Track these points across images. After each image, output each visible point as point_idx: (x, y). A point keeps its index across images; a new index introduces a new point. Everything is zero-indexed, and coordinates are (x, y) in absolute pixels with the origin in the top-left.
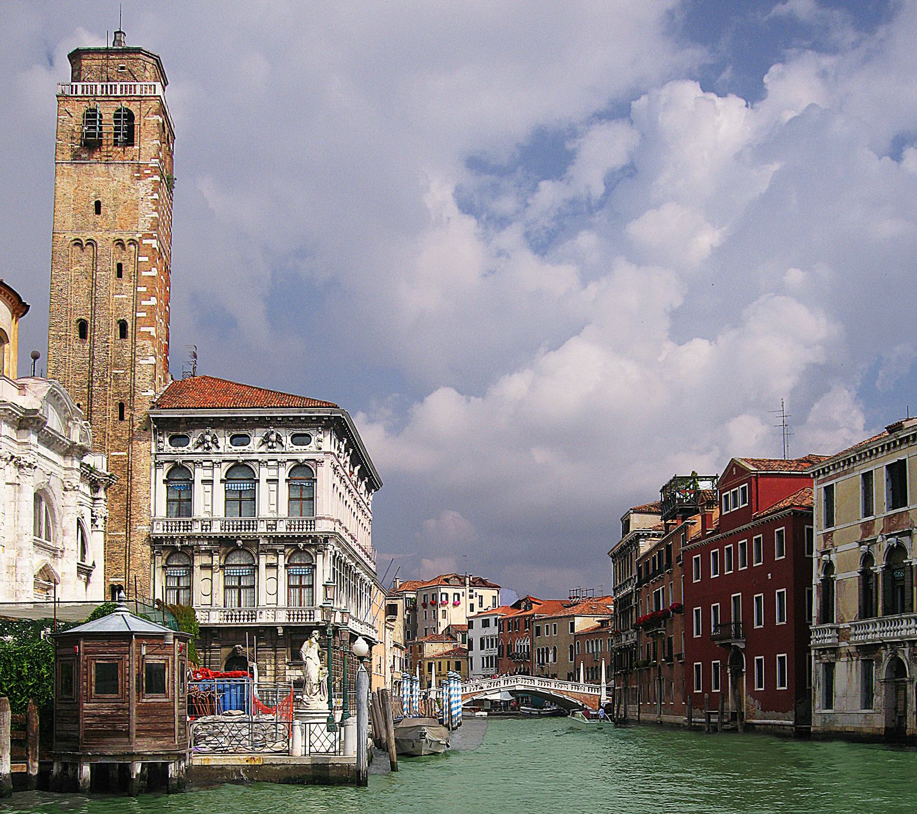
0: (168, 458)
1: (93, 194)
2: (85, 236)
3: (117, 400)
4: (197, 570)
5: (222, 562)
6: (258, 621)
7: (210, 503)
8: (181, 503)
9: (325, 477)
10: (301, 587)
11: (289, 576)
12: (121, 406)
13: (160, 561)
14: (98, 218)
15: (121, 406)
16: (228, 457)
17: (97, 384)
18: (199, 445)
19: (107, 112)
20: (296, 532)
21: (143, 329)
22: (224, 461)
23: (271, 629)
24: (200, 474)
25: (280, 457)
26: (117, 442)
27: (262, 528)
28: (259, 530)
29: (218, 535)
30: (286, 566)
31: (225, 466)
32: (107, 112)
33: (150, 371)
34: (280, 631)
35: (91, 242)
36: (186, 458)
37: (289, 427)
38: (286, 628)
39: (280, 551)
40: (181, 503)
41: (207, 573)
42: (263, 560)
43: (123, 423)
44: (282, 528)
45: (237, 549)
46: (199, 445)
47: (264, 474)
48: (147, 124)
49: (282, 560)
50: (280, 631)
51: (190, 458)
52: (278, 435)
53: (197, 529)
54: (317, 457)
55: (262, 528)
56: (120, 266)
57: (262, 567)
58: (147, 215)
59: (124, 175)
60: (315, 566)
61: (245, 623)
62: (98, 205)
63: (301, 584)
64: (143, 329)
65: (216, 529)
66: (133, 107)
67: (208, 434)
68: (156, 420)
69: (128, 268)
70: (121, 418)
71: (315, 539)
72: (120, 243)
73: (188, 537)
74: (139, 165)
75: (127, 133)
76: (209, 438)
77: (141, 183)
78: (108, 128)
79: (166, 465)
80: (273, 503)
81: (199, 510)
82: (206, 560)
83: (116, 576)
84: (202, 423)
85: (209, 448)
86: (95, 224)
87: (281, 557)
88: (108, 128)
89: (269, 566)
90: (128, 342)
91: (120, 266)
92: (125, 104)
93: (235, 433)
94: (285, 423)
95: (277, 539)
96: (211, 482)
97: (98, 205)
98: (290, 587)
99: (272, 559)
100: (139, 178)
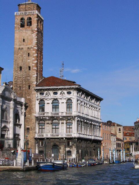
0: (39, 98)
1: (23, 38)
2: (22, 47)
4: (46, 124)
5: (51, 122)
7: (49, 109)
8: (42, 108)
9: (74, 101)
10: (69, 128)
11: (67, 125)
12: (29, 86)
13: (37, 122)
14: (24, 43)
15: (29, 86)
16: (53, 97)
18: (46, 95)
19: (26, 18)
20: (68, 115)
21: (34, 68)
22: (52, 98)
23: (62, 138)
24: (46, 102)
25: (64, 97)
26: (28, 95)
27: (60, 114)
30: (66, 123)
31: (52, 100)
32: (26, 18)
33: (35, 78)
34: (64, 139)
35: (22, 48)
36: (43, 98)
37: (66, 90)
38: (66, 138)
40: (42, 108)
41: (47, 125)
42: (61, 122)
44: (64, 114)
45: (55, 119)
46: (46, 95)
47: (60, 101)
48: (34, 20)
49: (65, 122)
50: (64, 139)
51: (44, 98)
52: (64, 92)
53: (46, 115)
54: (73, 97)
55: (60, 114)
56: (29, 54)
57: (60, 123)
58: (35, 41)
59: (29, 32)
60: (72, 123)
61: (56, 137)
62: (24, 40)
63: (69, 128)
64: (34, 68)
65: (50, 115)
66: (31, 17)
67: (48, 92)
68: (37, 89)
69: (31, 54)
70: (29, 89)
71: (72, 116)
72: (28, 48)
73: (44, 117)
74: (33, 30)
75: (30, 23)
76: (48, 93)
77: (33, 34)
78: (26, 22)
80: (62, 109)
81: (46, 110)
82: (47, 122)
83: (28, 126)
84: (46, 90)
85: (48, 95)
86: (23, 44)
87: (65, 121)
88: (26, 22)
89: (62, 123)
90: (31, 71)
91: (29, 54)
92: (29, 16)
93: (54, 91)
94: (65, 89)
96: (48, 103)
97: (24, 40)
98: (67, 128)
99: (63, 122)
100: (33, 33)
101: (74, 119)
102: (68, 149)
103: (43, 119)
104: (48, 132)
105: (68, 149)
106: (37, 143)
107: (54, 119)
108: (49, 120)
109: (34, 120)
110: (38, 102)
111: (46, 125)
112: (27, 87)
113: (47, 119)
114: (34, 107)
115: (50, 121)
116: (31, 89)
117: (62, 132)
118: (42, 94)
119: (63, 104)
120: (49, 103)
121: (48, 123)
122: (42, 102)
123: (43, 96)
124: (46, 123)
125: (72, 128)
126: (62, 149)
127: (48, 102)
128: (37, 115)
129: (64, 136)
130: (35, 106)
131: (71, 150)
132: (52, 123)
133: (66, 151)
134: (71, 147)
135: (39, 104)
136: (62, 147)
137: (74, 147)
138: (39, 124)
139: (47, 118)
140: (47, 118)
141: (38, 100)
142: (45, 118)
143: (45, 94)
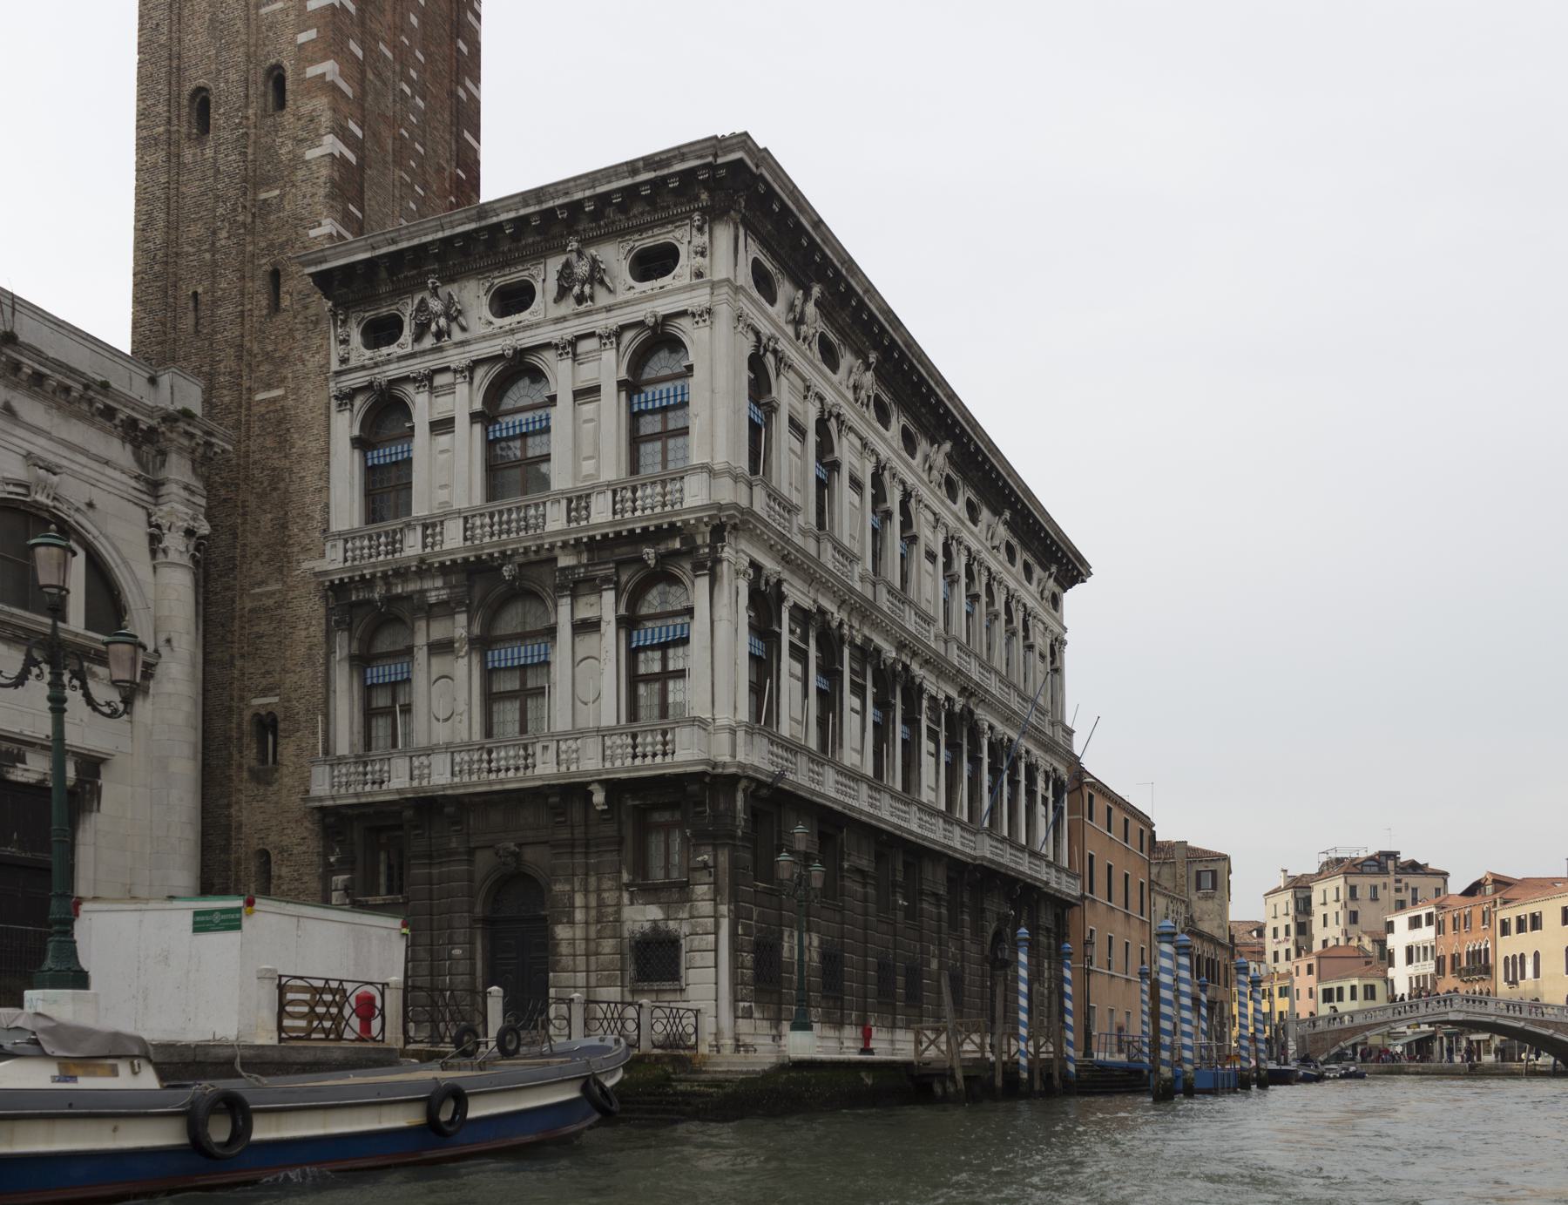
3: (265, 263)
4: (421, 655)
6: (539, 771)
8: (386, 488)
17: (224, 234)
23: (574, 792)
24: (423, 407)
26: (265, 368)
28: (551, 526)
29: (459, 557)
34: (599, 798)
36: (394, 371)
39: (606, 580)
40: (386, 488)
43: (279, 320)
49: (606, 606)
50: (599, 798)
61: (511, 780)
70: (275, 306)
73: (401, 573)
79: (359, 401)
83: (265, 692)
87: (609, 597)
95: (596, 546)
96: (442, 426)
101: (710, 567)
102: (642, 916)
103: (391, 600)
104: (444, 735)
105: (642, 916)
106: (346, 864)
107: (502, 594)
108: (445, 609)
109: (310, 610)
110: (344, 426)
111: (422, 668)
112: (258, 286)
113: (432, 598)
114: (312, 481)
115: (462, 619)
116: (286, 302)
117: (583, 715)
118: (381, 332)
119: (588, 409)
120: (442, 426)
121: (442, 648)
122: (385, 413)
123: (394, 349)
124: (420, 640)
125: (681, 674)
126: (579, 915)
127: (443, 406)
128: (333, 560)
129: (589, 761)
130: (325, 475)
131: (672, 925)
132: (482, 644)
133: (626, 934)
134: (676, 892)
135: (357, 443)
136: (579, 900)
137: (701, 890)
138: (361, 661)
139: (436, 590)
140: (427, 584)
141: (346, 398)
142: (412, 587)
143: (407, 334)
